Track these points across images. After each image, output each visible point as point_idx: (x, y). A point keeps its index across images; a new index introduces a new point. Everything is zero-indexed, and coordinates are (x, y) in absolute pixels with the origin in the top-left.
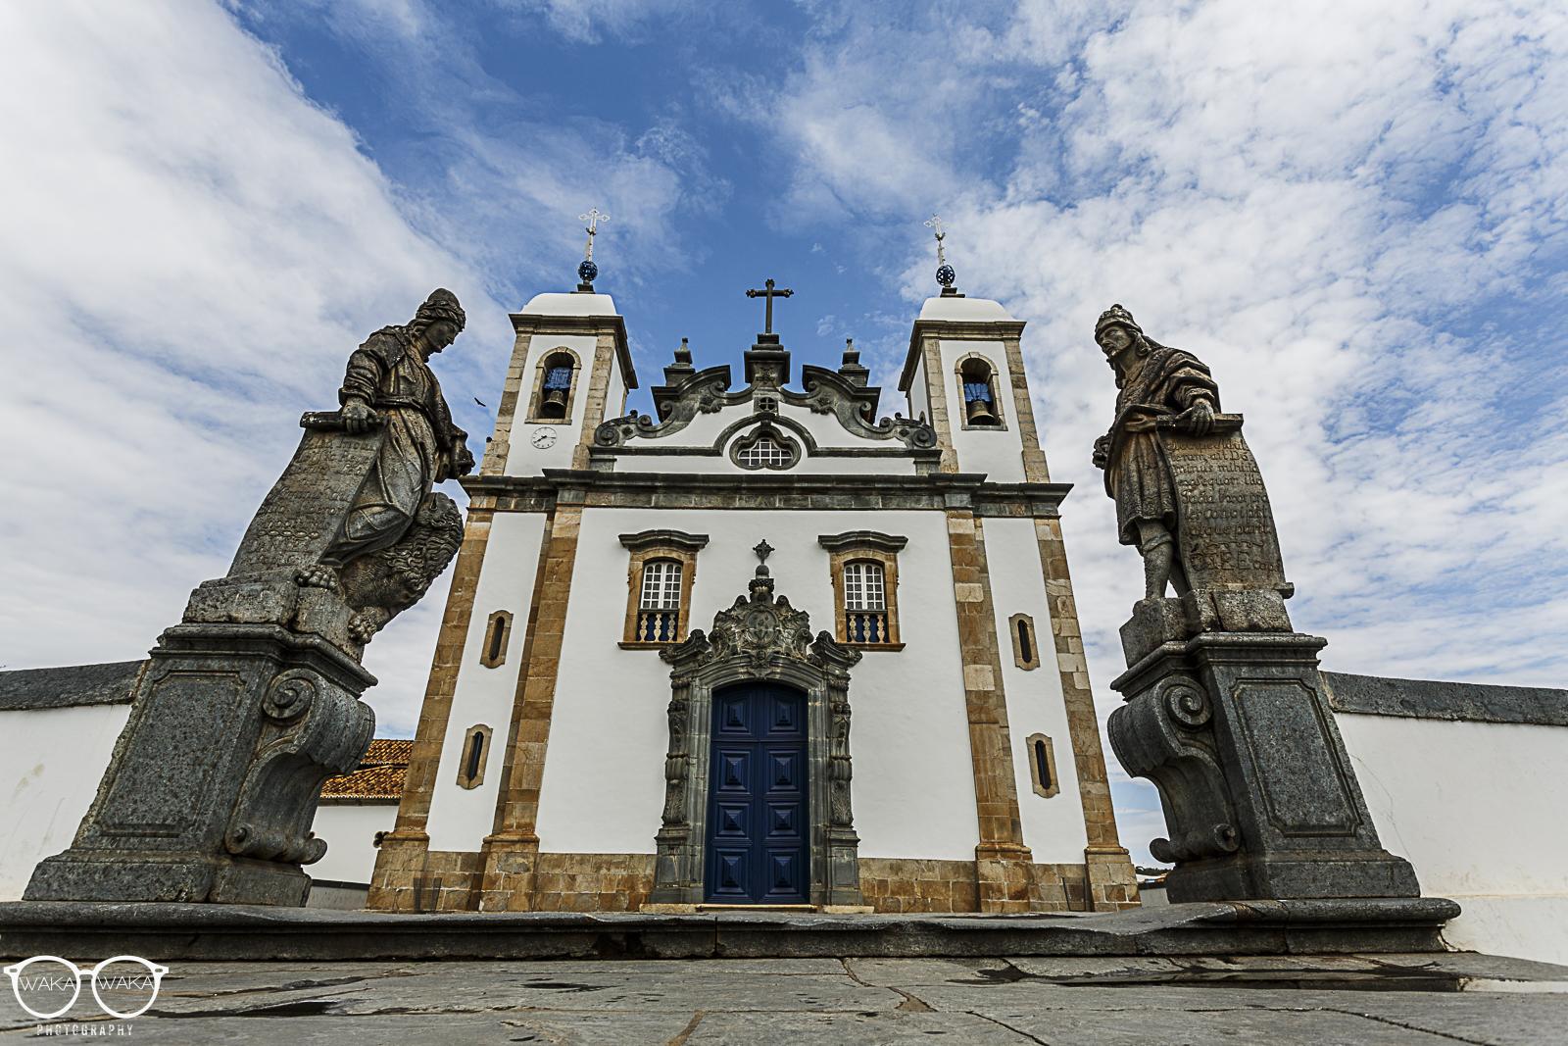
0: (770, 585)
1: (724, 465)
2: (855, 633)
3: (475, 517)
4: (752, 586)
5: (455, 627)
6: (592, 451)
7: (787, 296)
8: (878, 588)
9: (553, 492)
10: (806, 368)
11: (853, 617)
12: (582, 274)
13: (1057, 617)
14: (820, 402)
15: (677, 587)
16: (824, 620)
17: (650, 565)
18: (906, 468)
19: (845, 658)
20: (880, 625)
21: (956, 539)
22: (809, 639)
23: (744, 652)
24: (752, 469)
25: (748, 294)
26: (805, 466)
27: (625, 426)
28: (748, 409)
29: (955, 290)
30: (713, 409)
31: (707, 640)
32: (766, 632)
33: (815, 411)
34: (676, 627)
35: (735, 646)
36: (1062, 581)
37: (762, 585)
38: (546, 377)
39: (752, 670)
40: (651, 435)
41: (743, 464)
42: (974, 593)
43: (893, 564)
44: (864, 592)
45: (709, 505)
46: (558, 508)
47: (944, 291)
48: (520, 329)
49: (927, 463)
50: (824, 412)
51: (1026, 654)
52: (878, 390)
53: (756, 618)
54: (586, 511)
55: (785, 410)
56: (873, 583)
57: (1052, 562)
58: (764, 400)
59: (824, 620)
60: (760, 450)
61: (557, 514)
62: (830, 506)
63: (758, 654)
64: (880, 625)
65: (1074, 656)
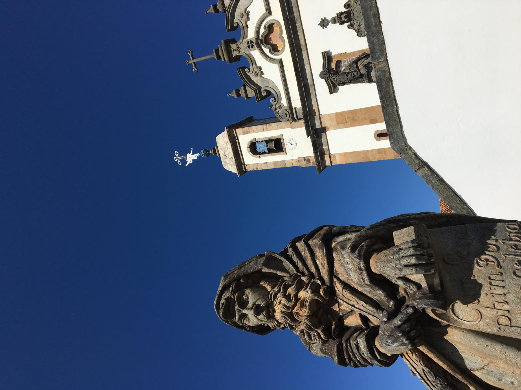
0: (341, 13)
1: (286, 56)
4: (343, 23)
5: (385, 154)
6: (294, 120)
26: (277, 15)
27: (278, 109)
28: (255, 53)
30: (260, 72)
33: (248, 19)
37: (339, 19)
40: (278, 96)
46: (323, 126)
48: (244, 171)
50: (248, 14)
55: (251, 34)
58: (249, 47)
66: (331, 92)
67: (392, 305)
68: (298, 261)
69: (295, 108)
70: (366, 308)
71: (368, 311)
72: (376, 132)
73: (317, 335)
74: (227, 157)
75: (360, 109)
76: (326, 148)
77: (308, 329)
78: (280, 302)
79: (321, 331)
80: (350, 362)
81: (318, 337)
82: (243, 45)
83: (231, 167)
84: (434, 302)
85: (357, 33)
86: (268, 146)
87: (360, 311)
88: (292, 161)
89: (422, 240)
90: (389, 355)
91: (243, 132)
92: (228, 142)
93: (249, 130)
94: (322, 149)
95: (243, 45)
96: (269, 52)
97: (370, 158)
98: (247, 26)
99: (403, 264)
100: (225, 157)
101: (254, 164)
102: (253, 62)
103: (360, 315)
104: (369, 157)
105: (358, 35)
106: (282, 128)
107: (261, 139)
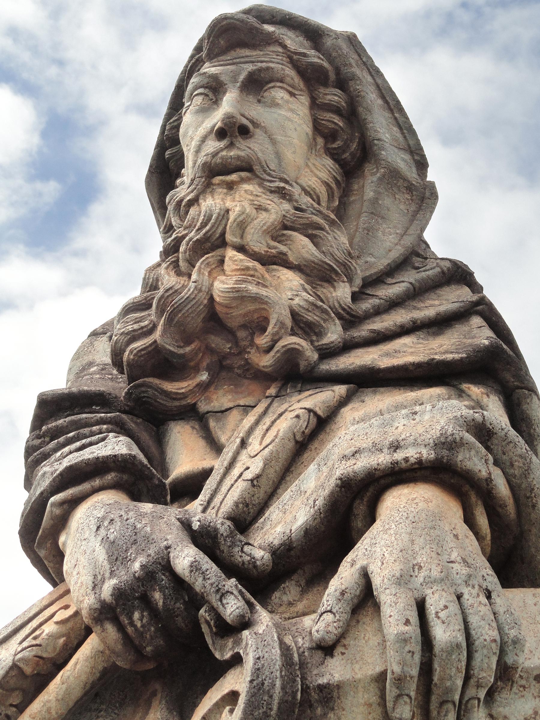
67: (250, 555)
68: (403, 282)
70: (236, 481)
71: (224, 489)
73: (142, 328)
77: (162, 297)
78: (260, 208)
79: (155, 341)
80: (44, 436)
81: (134, 331)
84: (271, 697)
87: (226, 463)
89: (523, 696)
90: (62, 539)
99: (429, 592)
103: (206, 473)
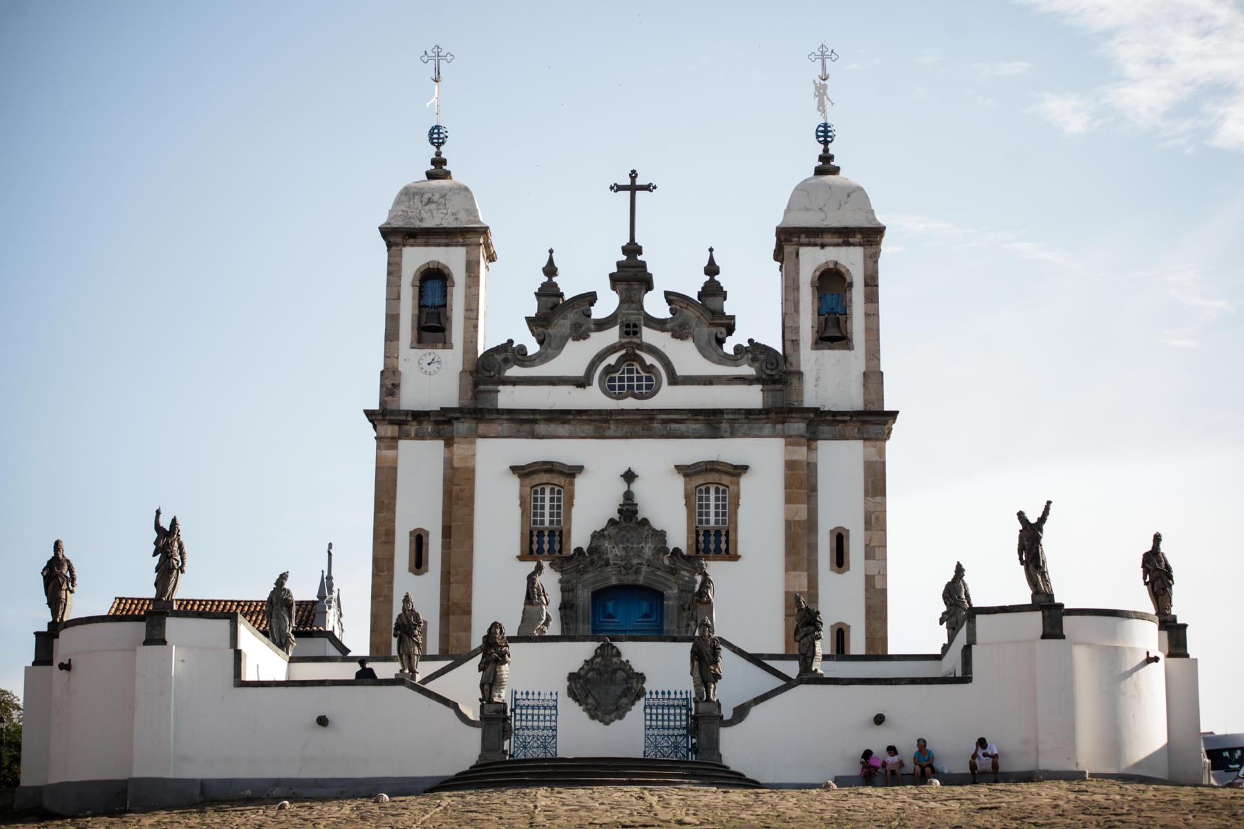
0: (636, 512)
2: (702, 546)
3: (382, 445)
4: (620, 511)
5: (385, 542)
6: (476, 384)
7: (651, 191)
8: (724, 507)
9: (449, 422)
10: (668, 295)
11: (701, 533)
12: (433, 143)
13: (870, 530)
14: (680, 327)
15: (559, 507)
16: (678, 538)
17: (535, 488)
18: (752, 397)
19: (692, 568)
20: (723, 539)
21: (790, 465)
22: (666, 550)
23: (615, 564)
24: (620, 397)
25: (612, 188)
26: (668, 397)
28: (612, 336)
29: (832, 157)
30: (580, 334)
31: (587, 554)
32: (632, 548)
34: (561, 542)
35: (608, 560)
36: (878, 499)
37: (628, 509)
38: (421, 292)
39: (622, 578)
40: (528, 363)
41: (609, 391)
42: (802, 512)
43: (736, 488)
44: (712, 510)
45: (583, 435)
47: (821, 158)
49: (772, 390)
51: (840, 560)
52: (733, 317)
53: (624, 536)
54: (481, 443)
56: (720, 503)
57: (872, 482)
58: (628, 326)
59: (678, 538)
60: (626, 375)
61: (455, 445)
62: (686, 434)
63: (626, 564)
64: (723, 539)
65: (879, 562)
66: (514, 469)
69: (499, 391)
72: (427, 533)
74: (426, 205)
75: (473, 514)
76: (411, 435)
82: (633, 314)
83: (402, 211)
85: (598, 530)
86: (433, 310)
88: (396, 356)
91: (472, 261)
92: (456, 219)
93: (474, 276)
94: (412, 425)
95: (633, 314)
96: (609, 365)
97: (380, 515)
98: (663, 330)
100: (427, 196)
101: (400, 270)
102: (602, 325)
104: (383, 513)
105: (595, 532)
106: (466, 352)
107: (452, 300)
